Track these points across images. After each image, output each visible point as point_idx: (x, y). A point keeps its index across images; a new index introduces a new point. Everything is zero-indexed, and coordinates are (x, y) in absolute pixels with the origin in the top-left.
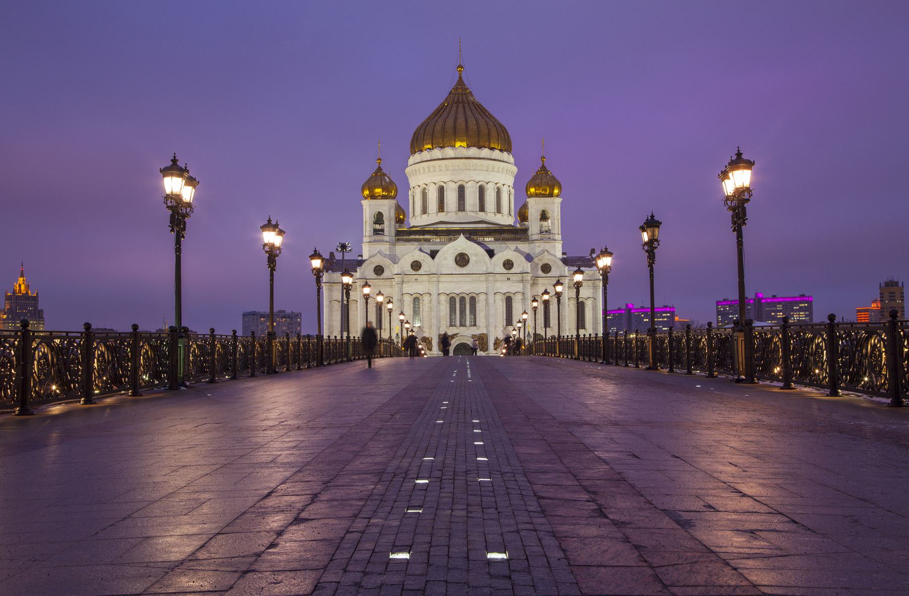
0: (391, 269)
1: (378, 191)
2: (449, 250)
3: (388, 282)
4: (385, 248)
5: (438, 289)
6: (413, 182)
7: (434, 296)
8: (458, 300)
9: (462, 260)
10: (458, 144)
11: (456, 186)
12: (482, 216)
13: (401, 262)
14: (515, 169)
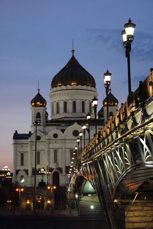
0: (44, 138)
1: (38, 103)
3: (42, 143)
5: (65, 146)
7: (64, 149)
9: (76, 133)
10: (73, 84)
11: (71, 102)
13: (49, 134)
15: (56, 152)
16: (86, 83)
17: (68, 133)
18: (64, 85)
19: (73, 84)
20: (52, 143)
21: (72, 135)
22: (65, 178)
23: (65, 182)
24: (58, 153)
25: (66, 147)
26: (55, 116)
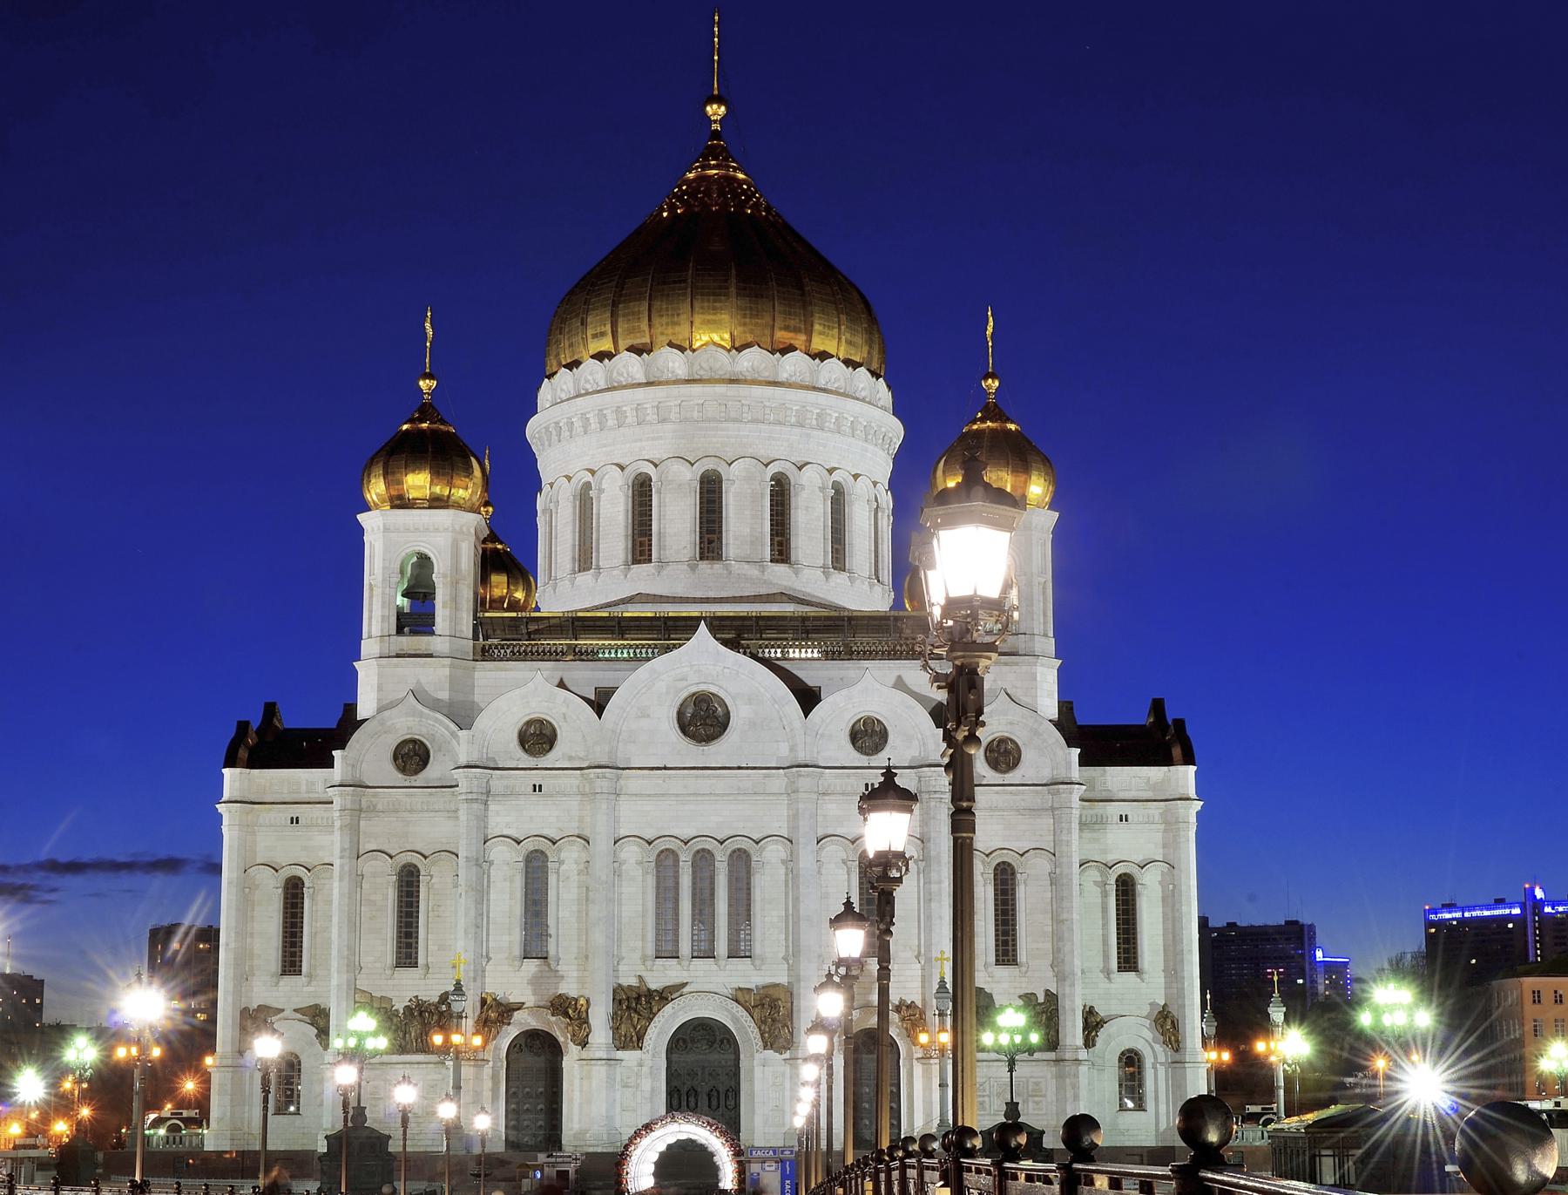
0: (454, 749)
1: (418, 482)
2: (657, 684)
3: (441, 798)
4: (434, 676)
5: (616, 821)
6: (548, 466)
8: (685, 858)
9: (703, 719)
10: (701, 338)
11: (689, 476)
12: (780, 576)
13: (481, 722)
14: (895, 430)
15: (536, 869)
16: (809, 334)
17: (644, 714)
18: (631, 349)
19: (705, 338)
20: (510, 794)
21: (675, 734)
22: (610, 1081)
23: (610, 1118)
24: (552, 879)
25: (623, 833)
26: (563, 586)
